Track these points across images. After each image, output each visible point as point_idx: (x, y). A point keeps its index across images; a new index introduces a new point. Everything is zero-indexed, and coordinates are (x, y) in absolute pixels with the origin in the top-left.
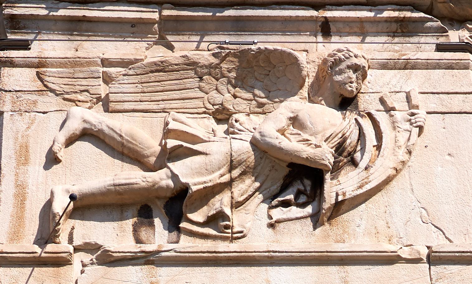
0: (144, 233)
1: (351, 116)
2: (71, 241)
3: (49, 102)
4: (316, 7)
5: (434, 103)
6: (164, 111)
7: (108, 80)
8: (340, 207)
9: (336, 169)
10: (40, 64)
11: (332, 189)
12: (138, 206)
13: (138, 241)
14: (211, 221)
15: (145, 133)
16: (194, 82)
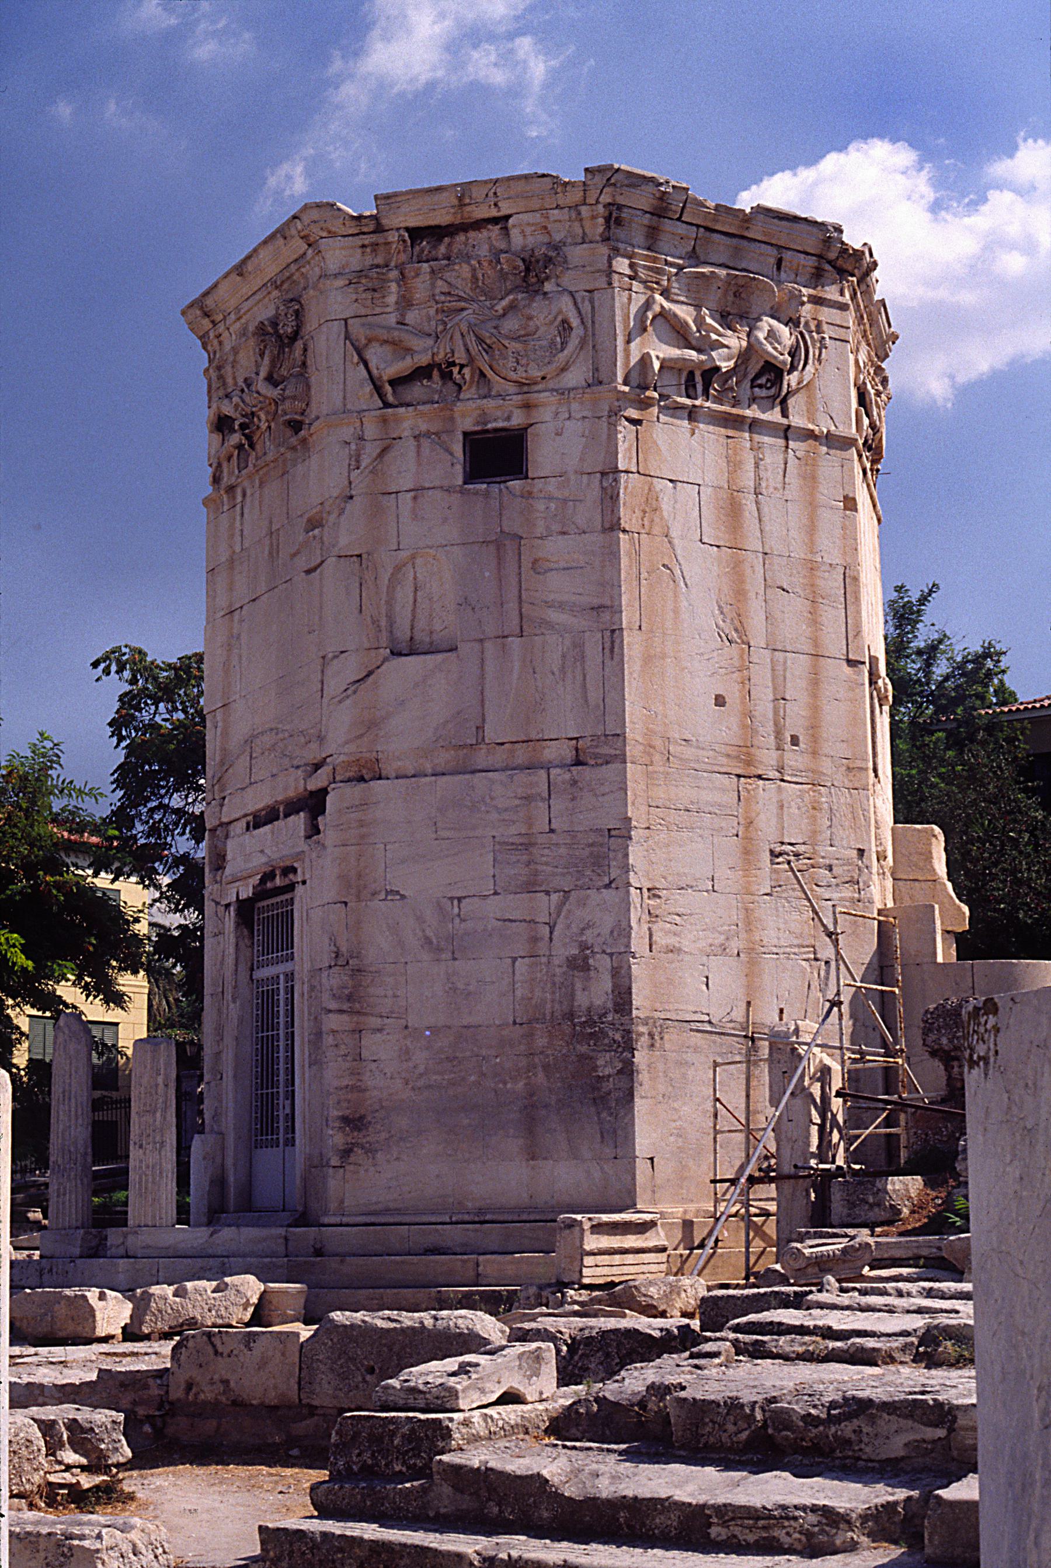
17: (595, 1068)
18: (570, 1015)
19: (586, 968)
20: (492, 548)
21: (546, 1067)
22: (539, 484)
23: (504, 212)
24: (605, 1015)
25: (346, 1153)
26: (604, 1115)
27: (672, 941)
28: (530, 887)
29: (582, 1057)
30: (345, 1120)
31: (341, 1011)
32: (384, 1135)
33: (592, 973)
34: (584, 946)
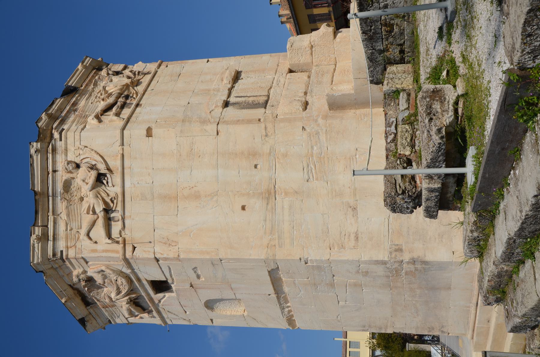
0: (116, 219)
1: (82, 165)
2: (119, 238)
3: (78, 245)
4: (48, 174)
5: (77, 143)
6: (81, 214)
7: (71, 230)
8: (109, 169)
9: (97, 169)
10: (67, 248)
11: (103, 170)
12: (108, 221)
13: (118, 221)
14: (112, 202)
15: (88, 219)
16: (72, 207)
17: (412, 272)
18: (388, 277)
24: (388, 268)
27: (353, 237)
33: (369, 270)
34: (358, 272)
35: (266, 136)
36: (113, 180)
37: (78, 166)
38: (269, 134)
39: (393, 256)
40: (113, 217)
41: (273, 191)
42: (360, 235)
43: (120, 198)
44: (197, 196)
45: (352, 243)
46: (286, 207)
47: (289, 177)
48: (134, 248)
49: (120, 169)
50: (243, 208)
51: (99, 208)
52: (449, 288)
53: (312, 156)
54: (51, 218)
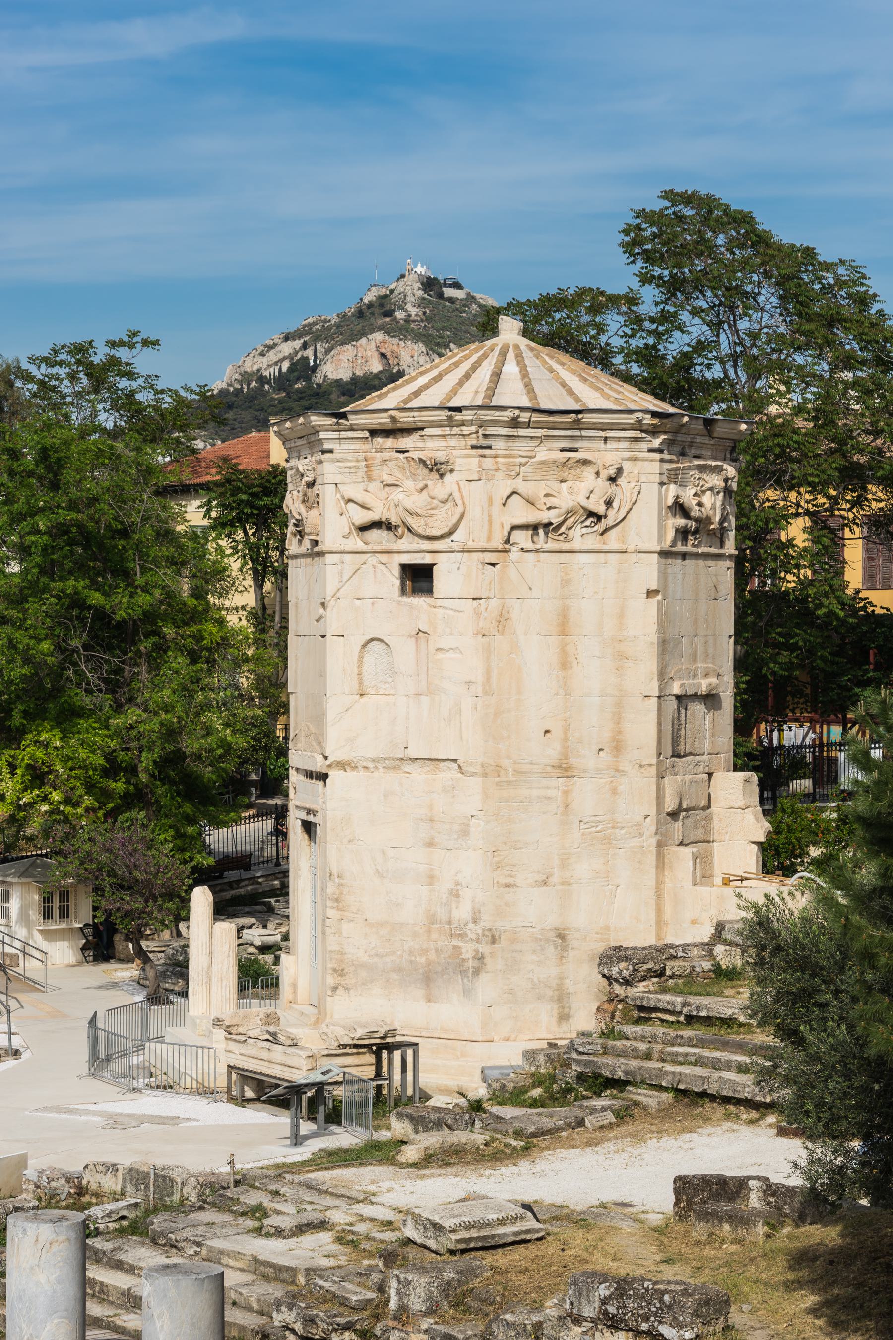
0: (535, 538)
17: (461, 954)
18: (450, 922)
19: (458, 896)
20: (413, 639)
21: (437, 950)
22: (439, 602)
23: (419, 425)
24: (466, 924)
25: (335, 989)
26: (465, 980)
27: (510, 880)
28: (430, 844)
29: (455, 947)
30: (335, 970)
31: (332, 907)
32: (353, 981)
34: (457, 884)
35: (641, 766)
36: (590, 536)
37: (612, 480)
38: (643, 770)
39: (487, 933)
40: (538, 534)
41: (569, 774)
42: (512, 890)
43: (566, 546)
44: (564, 665)
45: (503, 881)
46: (549, 792)
47: (587, 796)
48: (493, 565)
49: (606, 548)
50: (547, 731)
51: (553, 517)
52: (429, 1001)
53: (613, 828)
54: (539, 433)
